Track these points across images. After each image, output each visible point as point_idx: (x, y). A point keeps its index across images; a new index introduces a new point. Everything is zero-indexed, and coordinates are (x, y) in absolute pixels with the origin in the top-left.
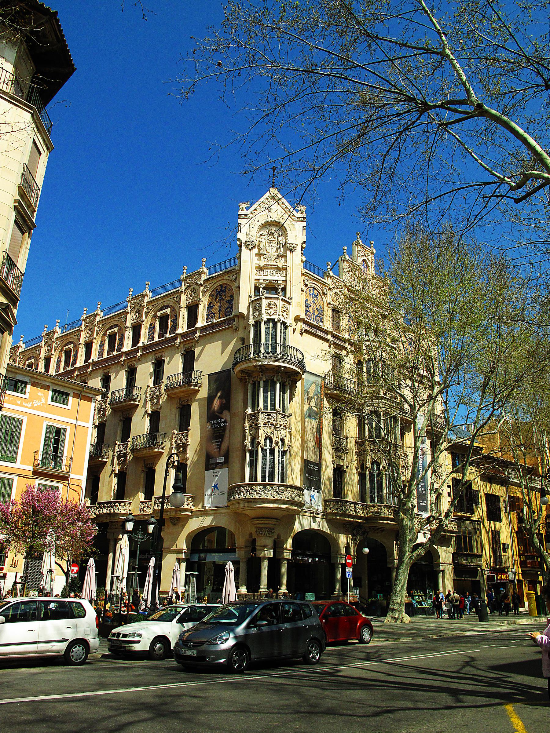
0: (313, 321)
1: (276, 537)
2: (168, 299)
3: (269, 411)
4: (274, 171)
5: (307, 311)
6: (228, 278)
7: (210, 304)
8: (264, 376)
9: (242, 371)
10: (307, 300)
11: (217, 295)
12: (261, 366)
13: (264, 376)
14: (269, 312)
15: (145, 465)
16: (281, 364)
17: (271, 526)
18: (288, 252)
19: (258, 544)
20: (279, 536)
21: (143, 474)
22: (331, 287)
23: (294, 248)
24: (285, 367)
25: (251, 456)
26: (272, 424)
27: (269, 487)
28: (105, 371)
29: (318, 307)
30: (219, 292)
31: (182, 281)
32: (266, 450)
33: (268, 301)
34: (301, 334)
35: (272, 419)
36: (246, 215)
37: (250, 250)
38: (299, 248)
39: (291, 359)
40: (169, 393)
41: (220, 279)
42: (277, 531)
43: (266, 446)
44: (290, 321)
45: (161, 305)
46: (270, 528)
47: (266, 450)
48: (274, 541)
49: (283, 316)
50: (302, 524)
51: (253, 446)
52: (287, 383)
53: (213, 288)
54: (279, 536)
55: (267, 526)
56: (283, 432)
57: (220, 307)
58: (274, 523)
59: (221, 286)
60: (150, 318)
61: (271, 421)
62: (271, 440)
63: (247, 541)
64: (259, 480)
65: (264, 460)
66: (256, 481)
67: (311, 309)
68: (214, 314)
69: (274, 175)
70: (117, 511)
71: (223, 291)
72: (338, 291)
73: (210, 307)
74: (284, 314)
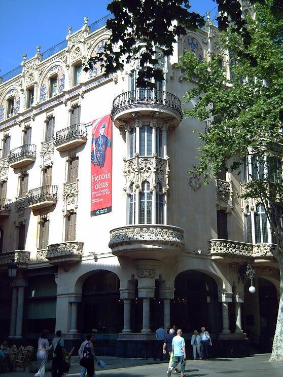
1: (158, 278)
2: (56, 60)
3: (146, 156)
9: (117, 119)
12: (136, 113)
13: (140, 123)
16: (156, 109)
19: (140, 285)
24: (160, 113)
25: (131, 200)
26: (149, 169)
27: (145, 229)
28: (6, 133)
31: (68, 41)
34: (180, 81)
40: (58, 147)
42: (158, 273)
43: (143, 189)
48: (156, 281)
51: (132, 191)
52: (164, 129)
54: (160, 276)
56: (160, 176)
61: (148, 165)
62: (148, 182)
63: (129, 281)
64: (137, 224)
65: (141, 203)
66: (134, 223)
68: (96, 69)
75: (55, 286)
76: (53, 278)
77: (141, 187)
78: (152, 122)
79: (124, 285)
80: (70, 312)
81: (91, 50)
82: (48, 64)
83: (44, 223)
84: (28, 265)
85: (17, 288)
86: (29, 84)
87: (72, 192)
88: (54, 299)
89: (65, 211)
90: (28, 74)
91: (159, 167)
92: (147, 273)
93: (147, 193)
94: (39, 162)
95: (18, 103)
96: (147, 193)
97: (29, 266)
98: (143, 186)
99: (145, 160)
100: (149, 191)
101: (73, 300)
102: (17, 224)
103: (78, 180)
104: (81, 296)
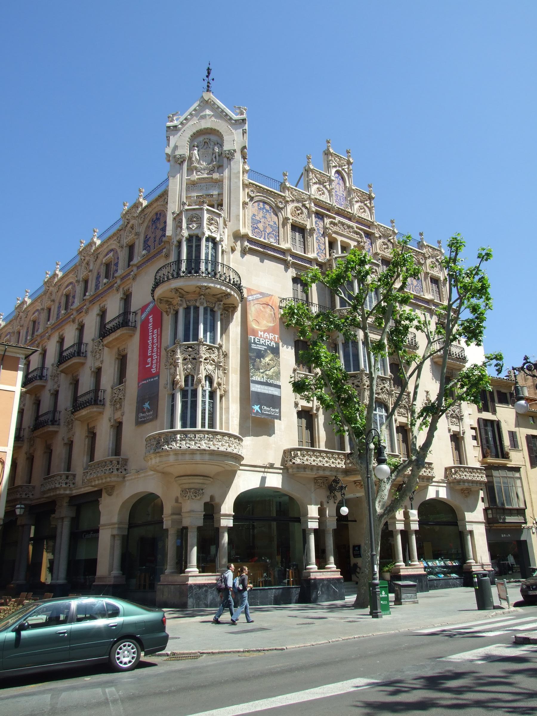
0: (264, 239)
4: (209, 73)
5: (254, 228)
6: (162, 203)
7: (146, 237)
8: (184, 301)
10: (254, 215)
11: (152, 224)
14: (191, 226)
15: (88, 429)
17: (198, 486)
18: (225, 160)
20: (212, 498)
21: (87, 440)
22: (288, 199)
23: (233, 155)
29: (272, 223)
30: (154, 221)
32: (187, 391)
33: (191, 213)
35: (195, 352)
36: (175, 127)
37: (180, 164)
38: (238, 156)
39: (225, 279)
41: (155, 205)
44: (225, 237)
45: (106, 251)
46: (196, 489)
47: (187, 391)
49: (209, 229)
50: (245, 482)
52: (216, 309)
53: (149, 218)
54: (212, 498)
55: (192, 486)
57: (155, 238)
58: (201, 481)
59: (157, 214)
60: (97, 267)
62: (193, 377)
67: (260, 226)
68: (149, 246)
69: (207, 77)
70: (57, 486)
71: (158, 219)
72: (300, 205)
73: (146, 241)
74: (212, 227)
75: (98, 514)
76: (96, 503)
77: (183, 383)
78: (198, 300)
79: (167, 510)
80: (112, 547)
81: (145, 224)
82: (105, 247)
83: (92, 436)
84: (72, 490)
85: (62, 519)
86: (85, 273)
87: (120, 396)
88: (97, 531)
89: (112, 421)
90: (85, 262)
91: (208, 355)
92: (191, 493)
93: (192, 390)
94: (90, 363)
95: (74, 297)
96: (192, 390)
97: (74, 492)
98: (186, 381)
99: (188, 347)
100: (192, 388)
101: (115, 532)
102: (66, 441)
103: (125, 382)
104: (127, 526)
